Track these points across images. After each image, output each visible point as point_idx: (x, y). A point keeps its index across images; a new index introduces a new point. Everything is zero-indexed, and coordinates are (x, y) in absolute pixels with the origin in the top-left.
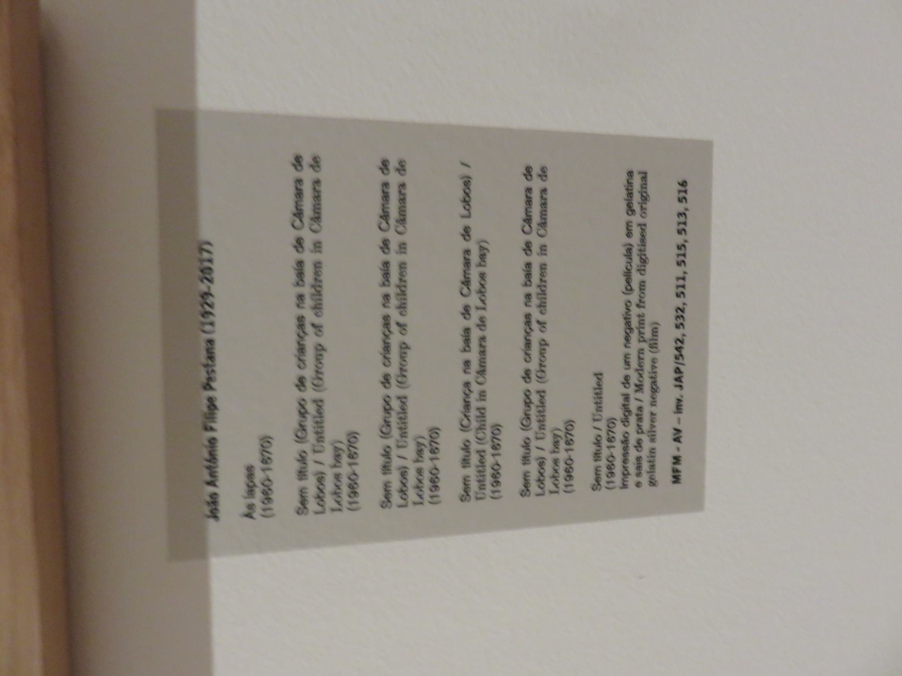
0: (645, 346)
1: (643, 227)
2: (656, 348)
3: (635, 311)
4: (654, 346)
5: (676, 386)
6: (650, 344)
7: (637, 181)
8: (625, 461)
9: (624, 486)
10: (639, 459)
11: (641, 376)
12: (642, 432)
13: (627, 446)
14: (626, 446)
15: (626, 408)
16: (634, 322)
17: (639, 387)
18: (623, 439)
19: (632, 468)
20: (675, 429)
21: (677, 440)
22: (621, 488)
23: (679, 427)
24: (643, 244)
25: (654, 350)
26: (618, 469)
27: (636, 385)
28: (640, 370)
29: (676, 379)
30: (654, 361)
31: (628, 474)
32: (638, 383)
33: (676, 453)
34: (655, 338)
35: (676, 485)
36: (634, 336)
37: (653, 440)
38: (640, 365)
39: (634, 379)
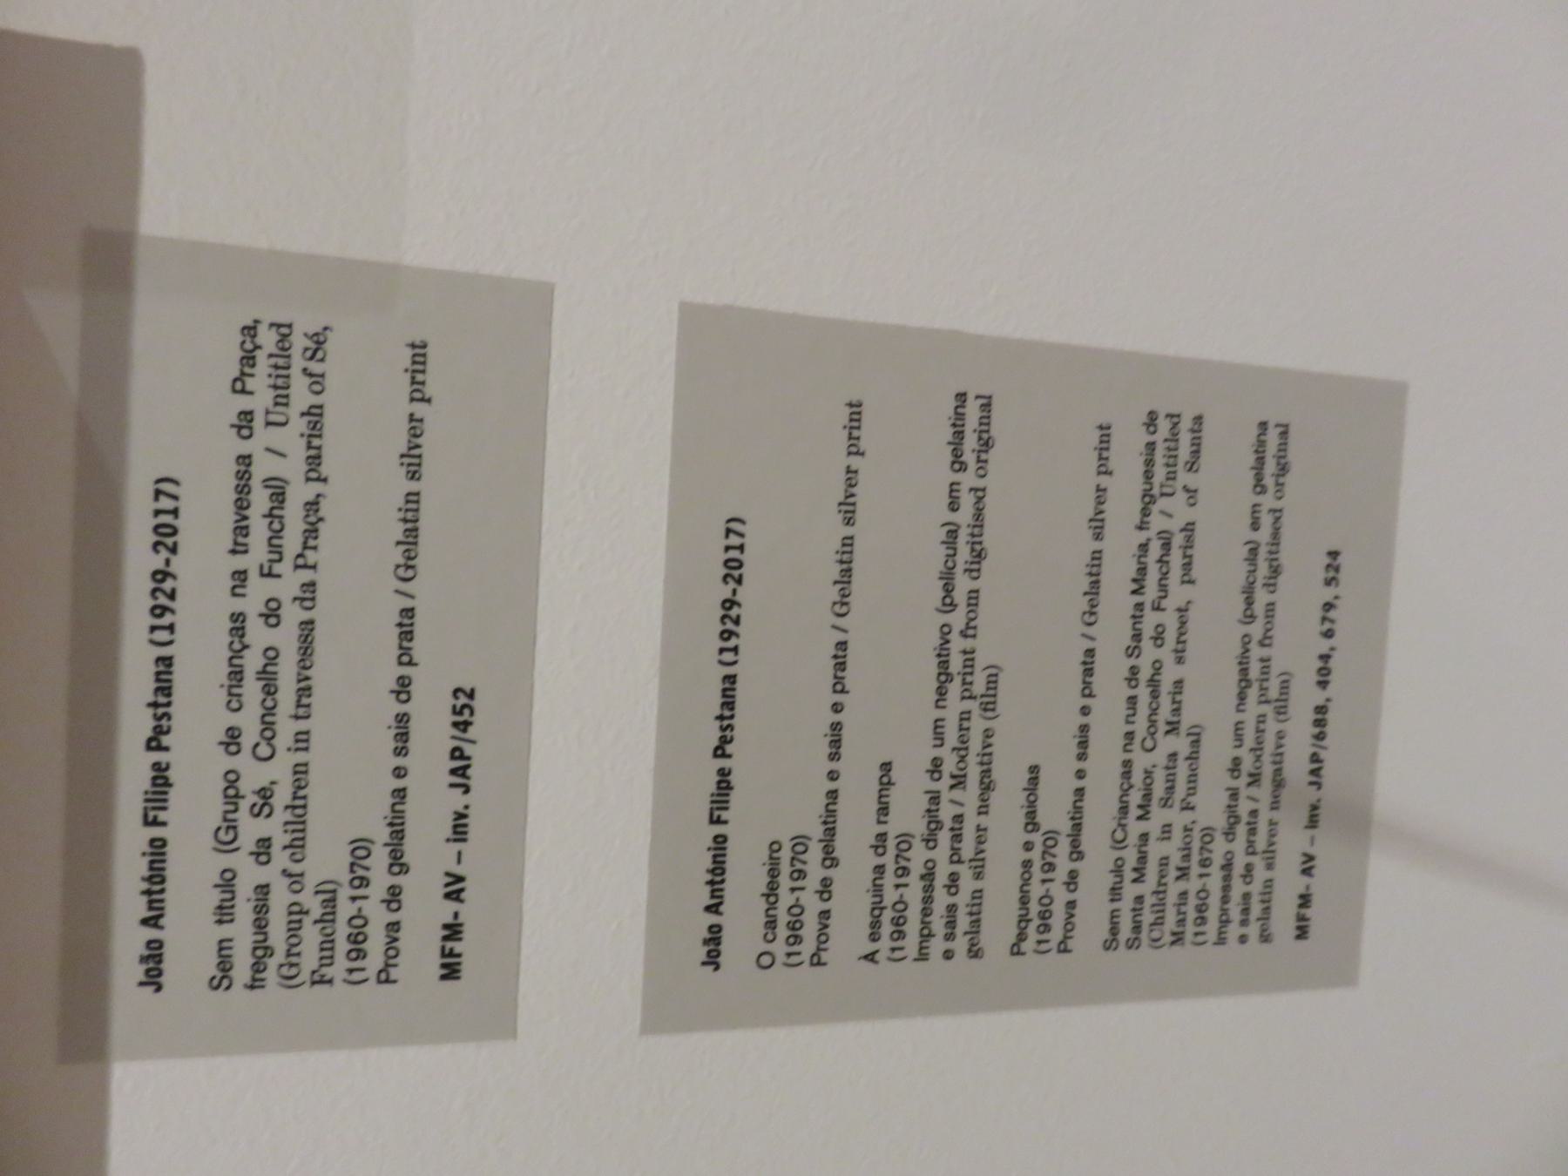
0: (973, 706)
1: (979, 494)
2: (993, 710)
3: (957, 644)
6: (981, 704)
7: (972, 412)
9: (923, 956)
11: (962, 759)
12: (959, 862)
14: (928, 883)
16: (956, 663)
17: (959, 781)
18: (924, 871)
19: (938, 924)
24: (978, 523)
25: (990, 714)
26: (913, 927)
27: (953, 777)
28: (962, 749)
30: (988, 734)
32: (956, 772)
34: (991, 692)
36: (955, 688)
38: (964, 741)
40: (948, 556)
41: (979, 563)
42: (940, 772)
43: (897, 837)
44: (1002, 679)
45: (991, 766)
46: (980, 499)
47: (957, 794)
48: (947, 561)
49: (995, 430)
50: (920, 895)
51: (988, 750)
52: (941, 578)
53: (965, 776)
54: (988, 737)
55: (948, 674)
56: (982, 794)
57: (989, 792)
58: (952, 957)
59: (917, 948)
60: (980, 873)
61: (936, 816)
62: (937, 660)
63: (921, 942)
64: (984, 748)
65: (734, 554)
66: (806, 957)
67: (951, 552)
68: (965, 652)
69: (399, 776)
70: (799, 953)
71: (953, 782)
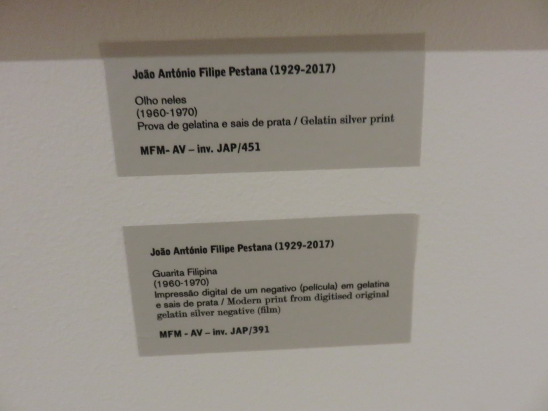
0: (263, 304)
1: (350, 296)
2: (262, 312)
3: (288, 294)
4: (264, 310)
5: (234, 329)
6: (264, 307)
8: (176, 295)
9: (157, 295)
10: (178, 305)
11: (241, 302)
12: (198, 306)
13: (187, 295)
14: (188, 294)
15: (217, 292)
16: (280, 295)
17: (232, 302)
18: (193, 292)
19: (170, 300)
20: (201, 330)
21: (193, 333)
22: (156, 293)
23: (203, 333)
24: (337, 297)
25: (260, 311)
26: (169, 289)
27: (233, 299)
28: (245, 301)
29: (239, 329)
30: (252, 311)
31: (166, 297)
32: (235, 300)
33: (183, 333)
34: (269, 311)
35: (159, 334)
36: (270, 295)
37: (192, 314)
39: (238, 297)
40: (324, 287)
41: (322, 299)
42: (235, 293)
43: (207, 279)
44: (275, 314)
45: (239, 314)
46: (347, 297)
47: (226, 302)
48: (321, 286)
49: (375, 300)
50: (183, 291)
51: (245, 312)
52: (314, 285)
53: (234, 303)
54: (251, 312)
55: (276, 292)
56: (227, 312)
57: (228, 315)
58: (158, 308)
59: (161, 292)
60: (194, 314)
61: (216, 294)
62: (281, 287)
63: (163, 294)
64: (246, 310)
65: (319, 69)
66: (142, 120)
67: (325, 287)
68: (285, 298)
69: (223, 125)
70: (143, 116)
71: (231, 299)
